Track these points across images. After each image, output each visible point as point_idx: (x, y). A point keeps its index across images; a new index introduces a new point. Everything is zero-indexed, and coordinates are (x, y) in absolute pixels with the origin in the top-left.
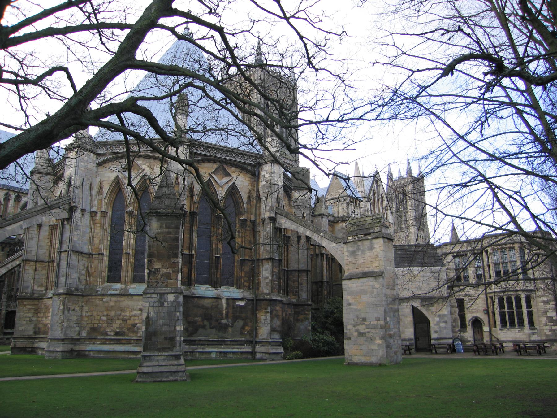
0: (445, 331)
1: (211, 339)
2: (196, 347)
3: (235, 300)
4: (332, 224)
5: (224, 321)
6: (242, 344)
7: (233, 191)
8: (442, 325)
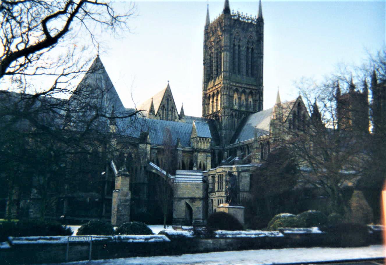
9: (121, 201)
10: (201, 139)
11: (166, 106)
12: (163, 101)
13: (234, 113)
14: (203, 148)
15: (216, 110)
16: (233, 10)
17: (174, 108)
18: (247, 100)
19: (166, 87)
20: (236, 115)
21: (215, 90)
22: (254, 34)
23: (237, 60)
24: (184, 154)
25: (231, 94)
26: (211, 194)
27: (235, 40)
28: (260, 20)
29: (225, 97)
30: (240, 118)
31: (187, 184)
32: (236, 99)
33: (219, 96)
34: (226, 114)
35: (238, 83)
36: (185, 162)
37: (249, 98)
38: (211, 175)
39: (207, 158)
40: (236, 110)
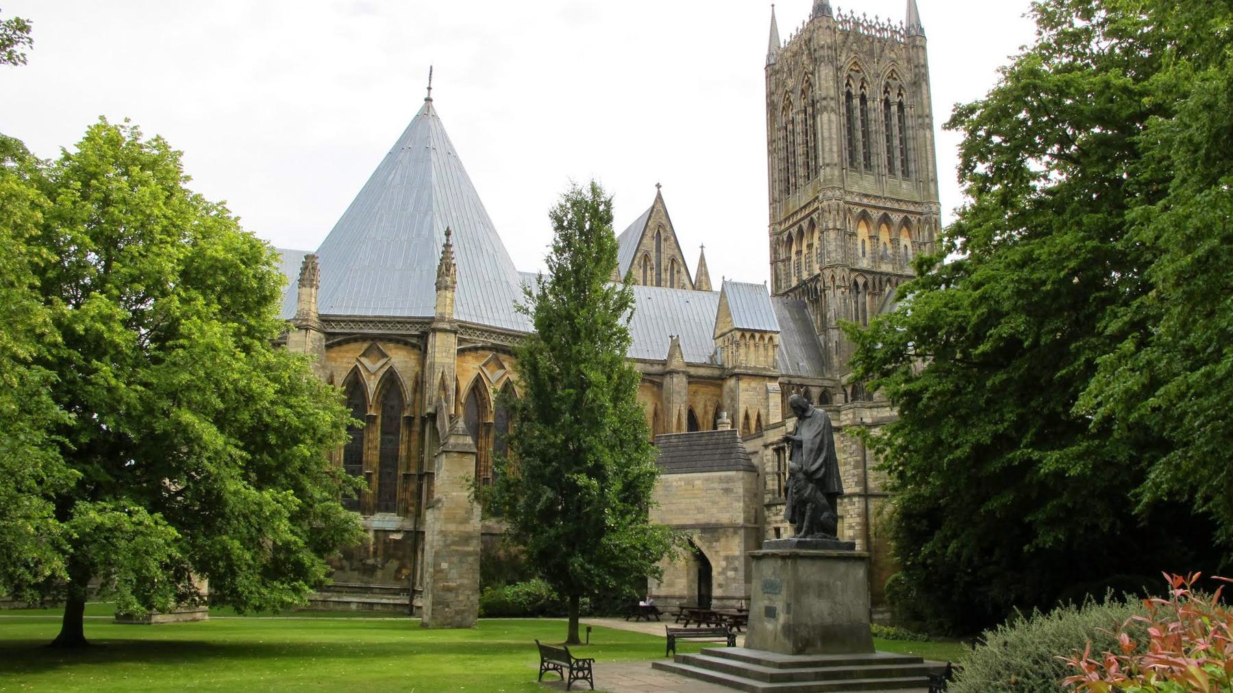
0: (734, 585)
2: (329, 594)
3: (386, 532)
4: (719, 382)
5: (371, 561)
6: (396, 593)
7: (390, 380)
8: (731, 574)
9: (445, 541)
10: (748, 335)
11: (653, 255)
12: (644, 241)
13: (861, 281)
14: (753, 364)
15: (809, 275)
16: (839, 10)
17: (677, 261)
18: (895, 242)
19: (650, 203)
20: (865, 285)
21: (802, 219)
22: (902, 64)
23: (859, 135)
24: (694, 387)
25: (851, 227)
26: (773, 509)
27: (851, 82)
28: (914, 38)
29: (832, 234)
30: (880, 295)
31: (693, 480)
32: (863, 241)
33: (816, 234)
34: (837, 283)
35: (866, 196)
36: (699, 412)
37: (902, 237)
38: (772, 444)
39: (767, 398)
40: (863, 272)
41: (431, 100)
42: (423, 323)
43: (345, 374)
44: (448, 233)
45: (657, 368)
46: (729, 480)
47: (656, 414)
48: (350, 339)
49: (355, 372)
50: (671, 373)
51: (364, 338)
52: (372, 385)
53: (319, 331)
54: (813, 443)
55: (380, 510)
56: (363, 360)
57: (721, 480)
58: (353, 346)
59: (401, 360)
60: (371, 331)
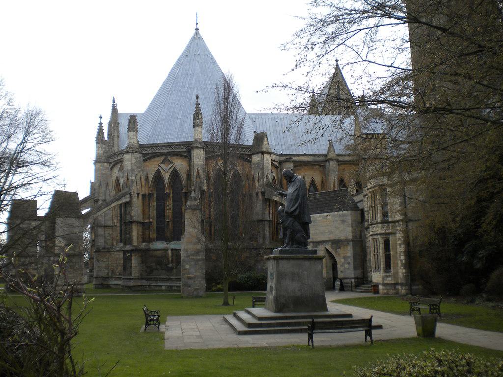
1: (161, 277)
5: (170, 265)
7: (175, 174)
8: (346, 265)
9: (187, 254)
24: (342, 167)
41: (198, 30)
42: (189, 145)
43: (153, 173)
44: (197, 98)
45: (322, 158)
46: (344, 216)
47: (322, 182)
48: (155, 155)
49: (158, 172)
50: (328, 160)
51: (161, 154)
52: (166, 177)
53: (139, 152)
54: (292, 196)
55: (174, 240)
56: (162, 165)
57: (340, 216)
58: (157, 159)
59: (179, 164)
60: (164, 151)
